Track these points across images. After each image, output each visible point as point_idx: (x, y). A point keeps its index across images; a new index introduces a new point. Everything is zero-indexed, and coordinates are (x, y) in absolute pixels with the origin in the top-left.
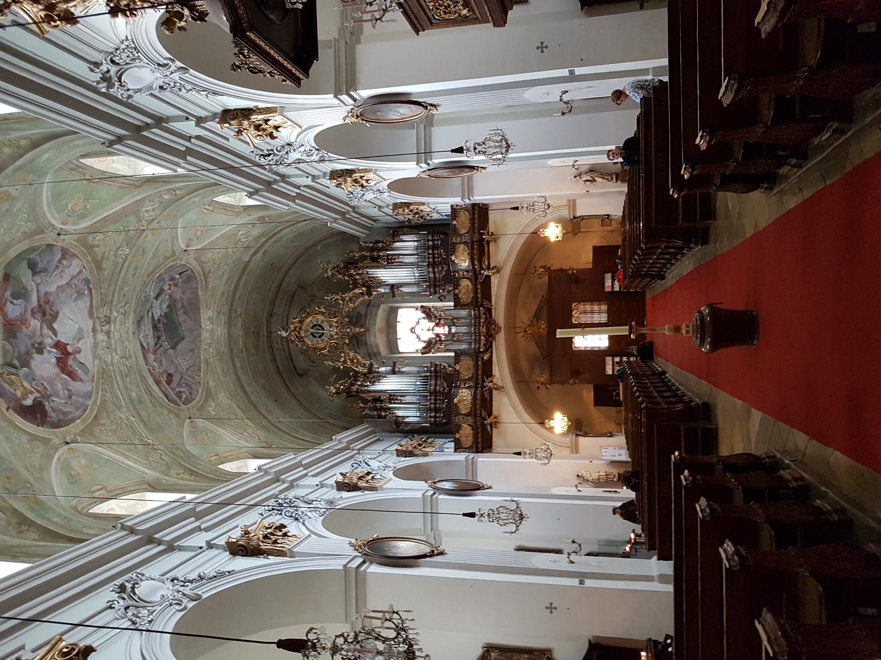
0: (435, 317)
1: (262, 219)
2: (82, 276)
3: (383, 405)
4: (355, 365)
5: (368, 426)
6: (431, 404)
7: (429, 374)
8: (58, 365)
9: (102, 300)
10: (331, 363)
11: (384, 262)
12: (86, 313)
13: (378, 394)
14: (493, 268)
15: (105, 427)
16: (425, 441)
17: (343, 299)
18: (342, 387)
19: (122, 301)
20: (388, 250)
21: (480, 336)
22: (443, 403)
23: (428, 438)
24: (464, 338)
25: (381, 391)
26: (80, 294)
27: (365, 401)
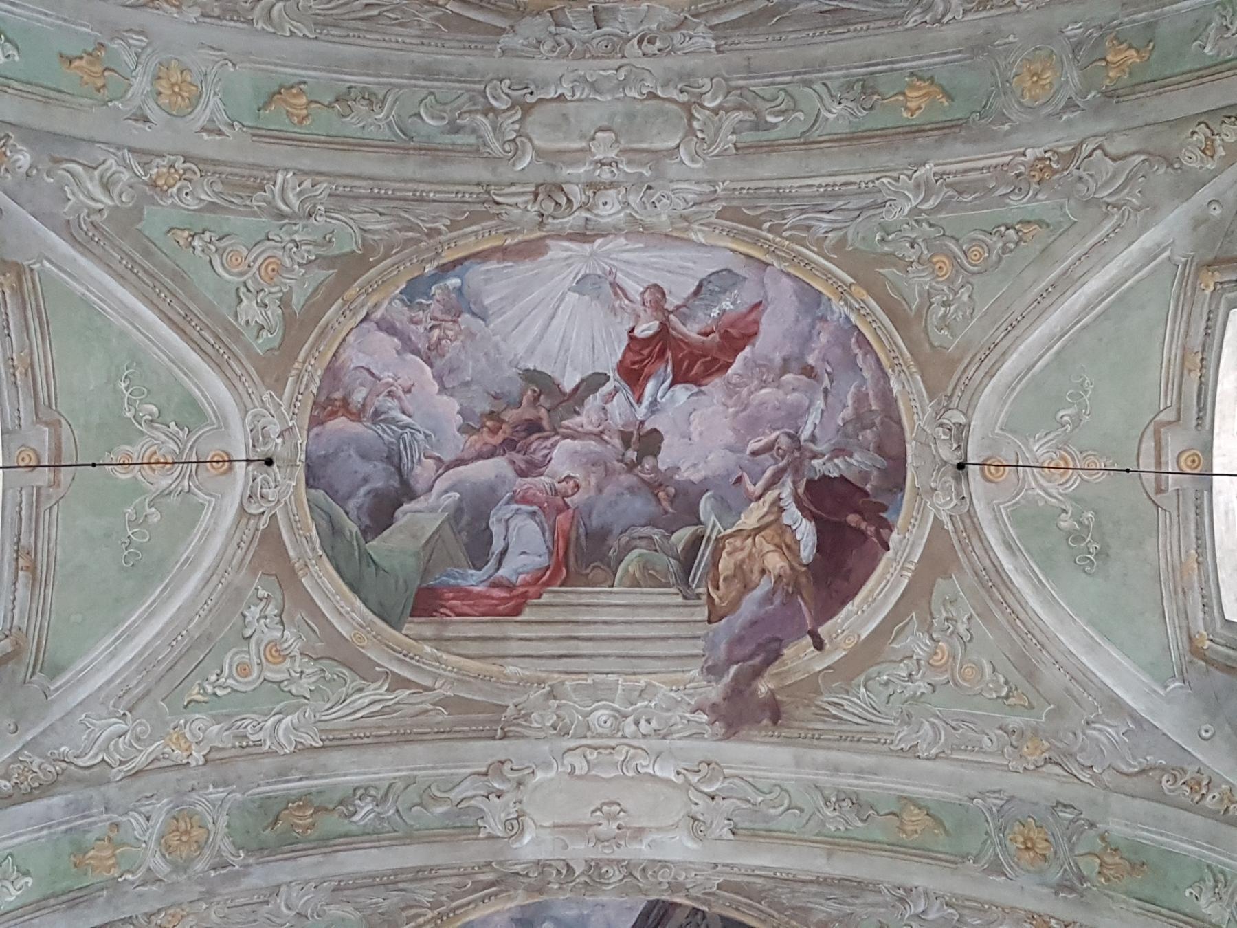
2: (400, 313)
8: (697, 381)
9: (474, 218)
12: (525, 268)
15: (937, 299)
19: (474, 131)
26: (461, 305)
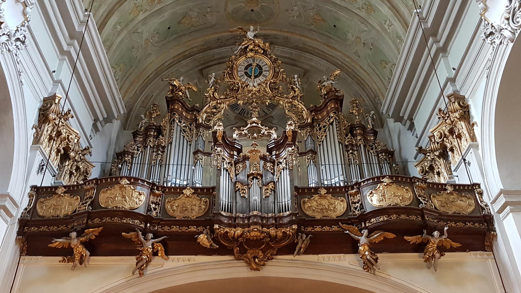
0: (278, 156)
5: (122, 112)
10: (212, 81)
11: (348, 142)
13: (168, 133)
16: (78, 169)
17: (293, 98)
18: (181, 94)
20: (365, 146)
21: (243, 226)
25: (171, 136)
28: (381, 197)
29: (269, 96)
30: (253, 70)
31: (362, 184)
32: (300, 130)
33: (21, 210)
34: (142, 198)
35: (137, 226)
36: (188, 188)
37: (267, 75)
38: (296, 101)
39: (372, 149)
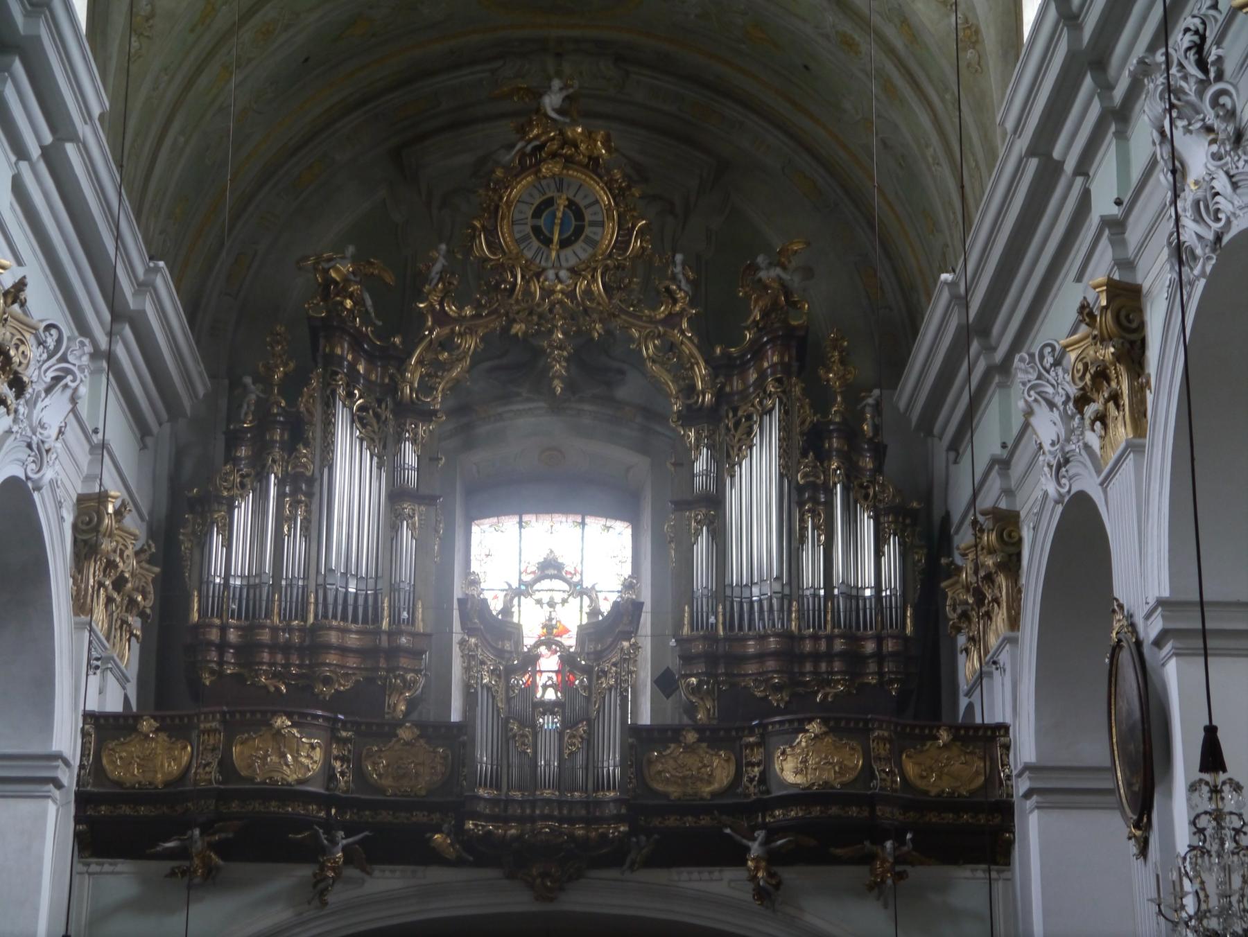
1: (968, 36)
3: (277, 453)
4: (429, 356)
5: (201, 391)
6: (274, 630)
7: (385, 624)
10: (438, 267)
11: (805, 476)
13: (319, 434)
14: (771, 875)
16: (132, 602)
17: (672, 320)
18: (349, 303)
20: (846, 490)
21: (521, 820)
22: (275, 675)
23: (142, 614)
24: (515, 760)
27: (294, 385)
28: (799, 765)
29: (602, 312)
30: (558, 221)
31: (770, 727)
32: (682, 425)
33: (76, 771)
34: (318, 755)
35: (314, 817)
36: (407, 724)
37: (597, 238)
38: (676, 331)
39: (866, 497)
